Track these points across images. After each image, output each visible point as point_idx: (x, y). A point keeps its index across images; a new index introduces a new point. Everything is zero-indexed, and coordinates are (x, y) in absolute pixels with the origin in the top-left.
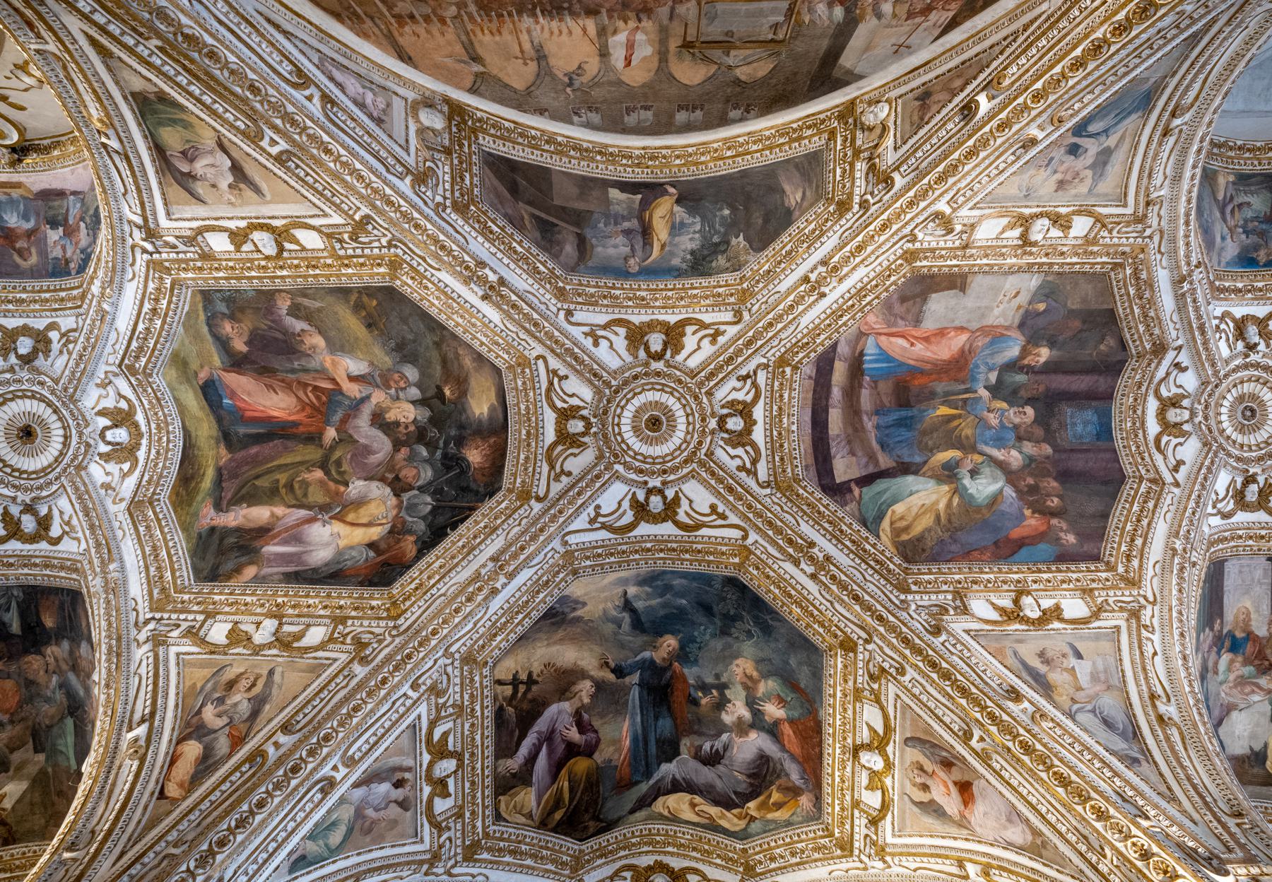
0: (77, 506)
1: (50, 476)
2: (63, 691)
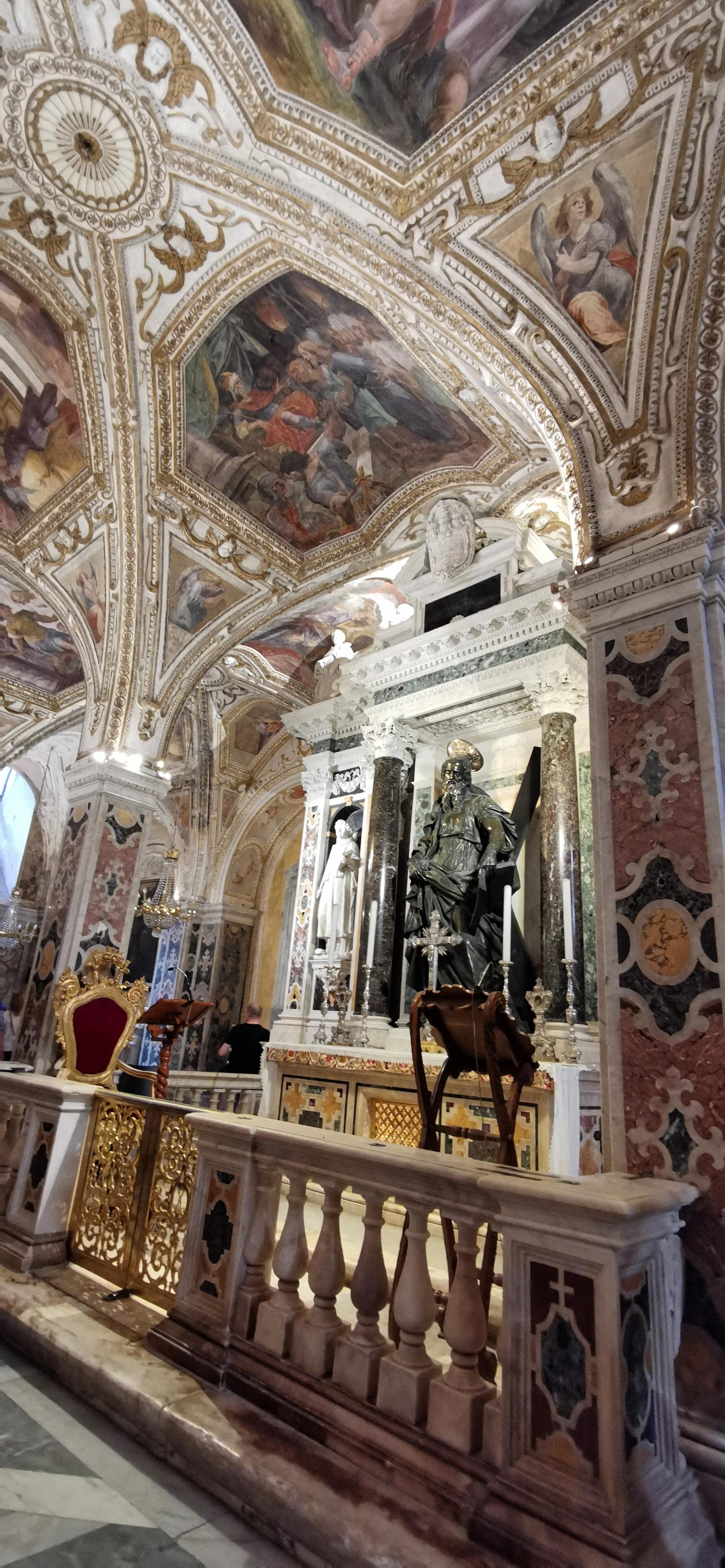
0: (208, 184)
1: (150, 177)
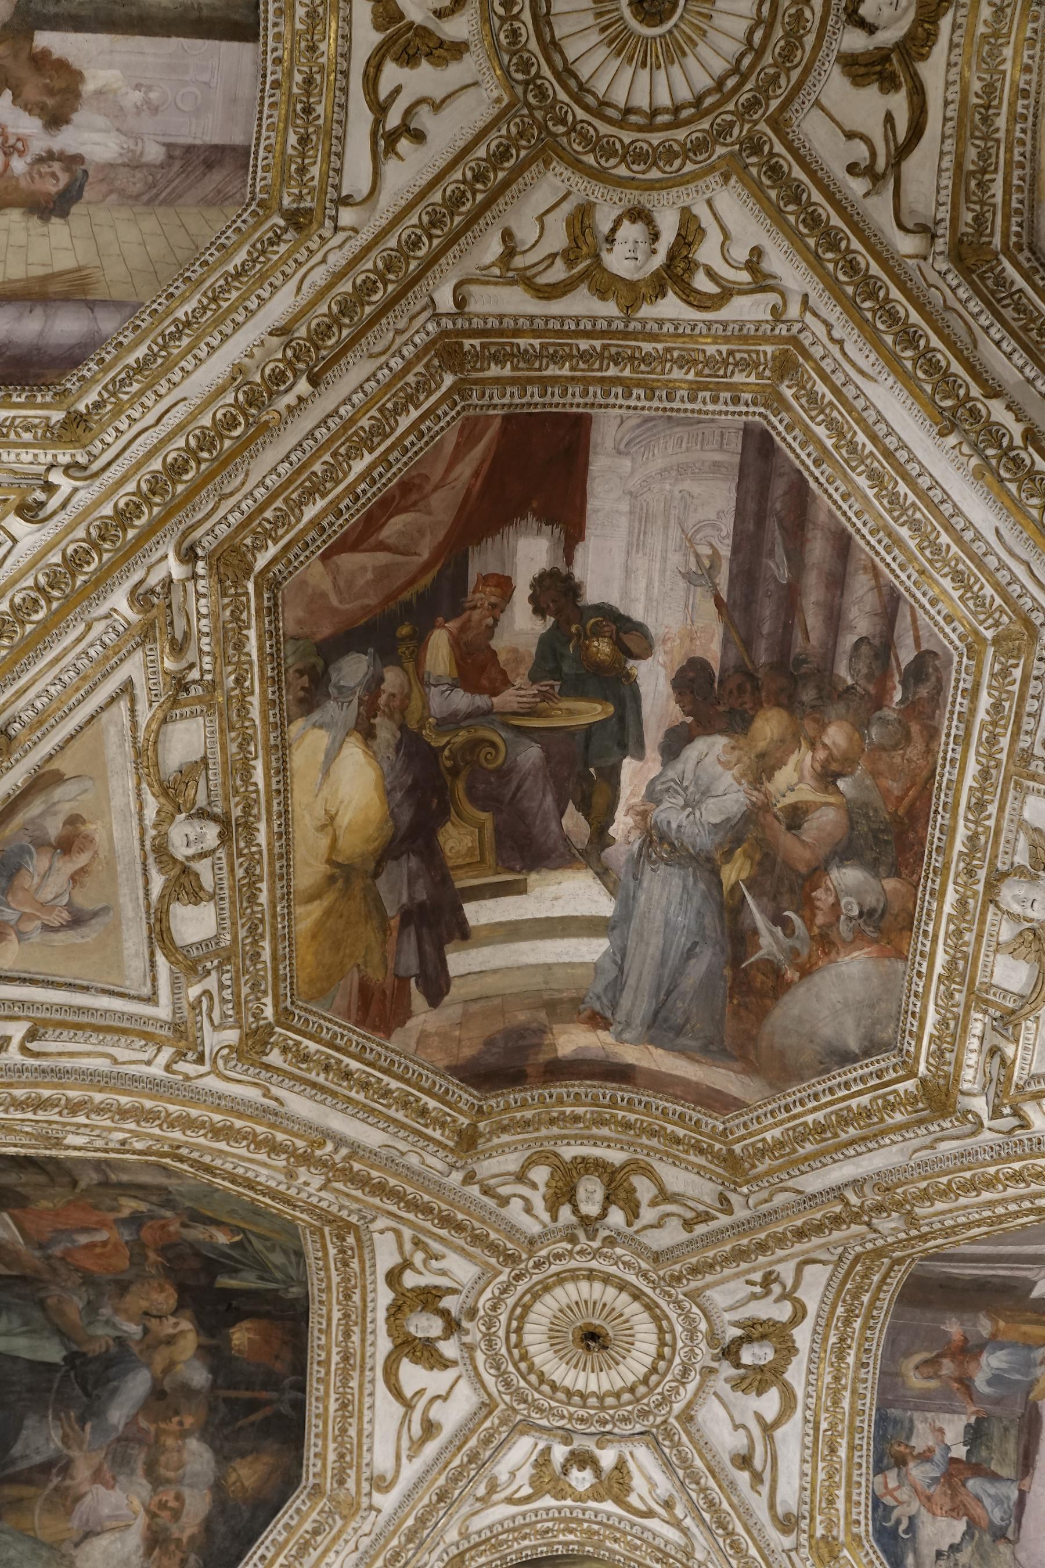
2: (114, 1350)
